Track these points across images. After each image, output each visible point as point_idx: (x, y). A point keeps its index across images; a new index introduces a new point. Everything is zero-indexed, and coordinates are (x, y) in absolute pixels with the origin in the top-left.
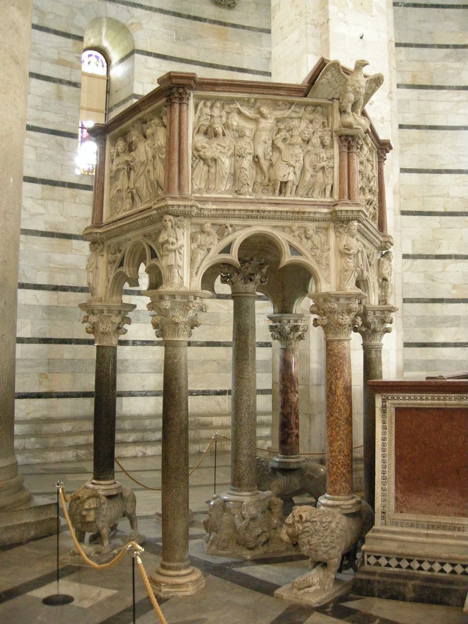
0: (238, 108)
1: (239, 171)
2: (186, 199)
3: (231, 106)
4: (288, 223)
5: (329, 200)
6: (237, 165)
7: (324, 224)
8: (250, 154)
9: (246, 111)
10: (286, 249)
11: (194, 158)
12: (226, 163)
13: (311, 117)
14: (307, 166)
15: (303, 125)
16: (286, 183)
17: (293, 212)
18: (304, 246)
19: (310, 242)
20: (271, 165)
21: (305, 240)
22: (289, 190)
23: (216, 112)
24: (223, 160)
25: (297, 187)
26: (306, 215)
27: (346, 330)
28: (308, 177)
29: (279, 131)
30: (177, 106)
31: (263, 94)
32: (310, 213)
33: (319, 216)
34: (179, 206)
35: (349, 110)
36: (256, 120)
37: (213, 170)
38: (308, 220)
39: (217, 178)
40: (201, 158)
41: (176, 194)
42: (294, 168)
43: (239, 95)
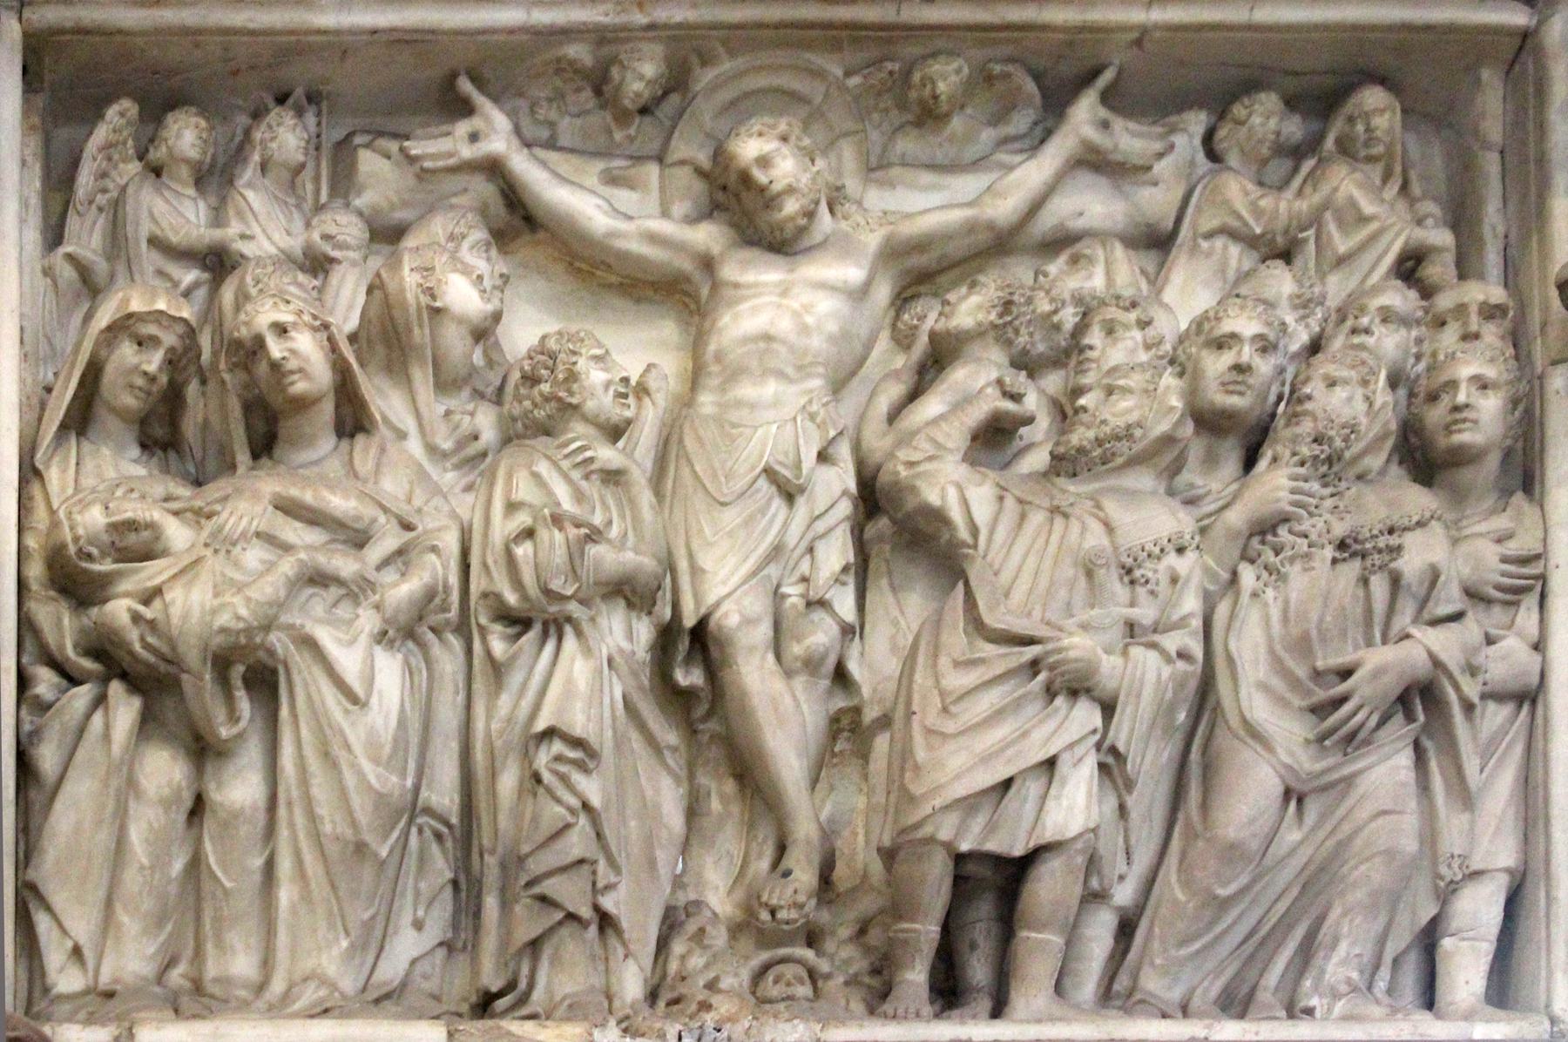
0: (494, 168)
1: (508, 781)
3: (415, 148)
6: (500, 714)
9: (578, 197)
12: (368, 693)
13: (1286, 206)
14: (1254, 695)
16: (1012, 874)
23: (264, 226)
29: (937, 360)
39: (285, 866)
40: (110, 661)
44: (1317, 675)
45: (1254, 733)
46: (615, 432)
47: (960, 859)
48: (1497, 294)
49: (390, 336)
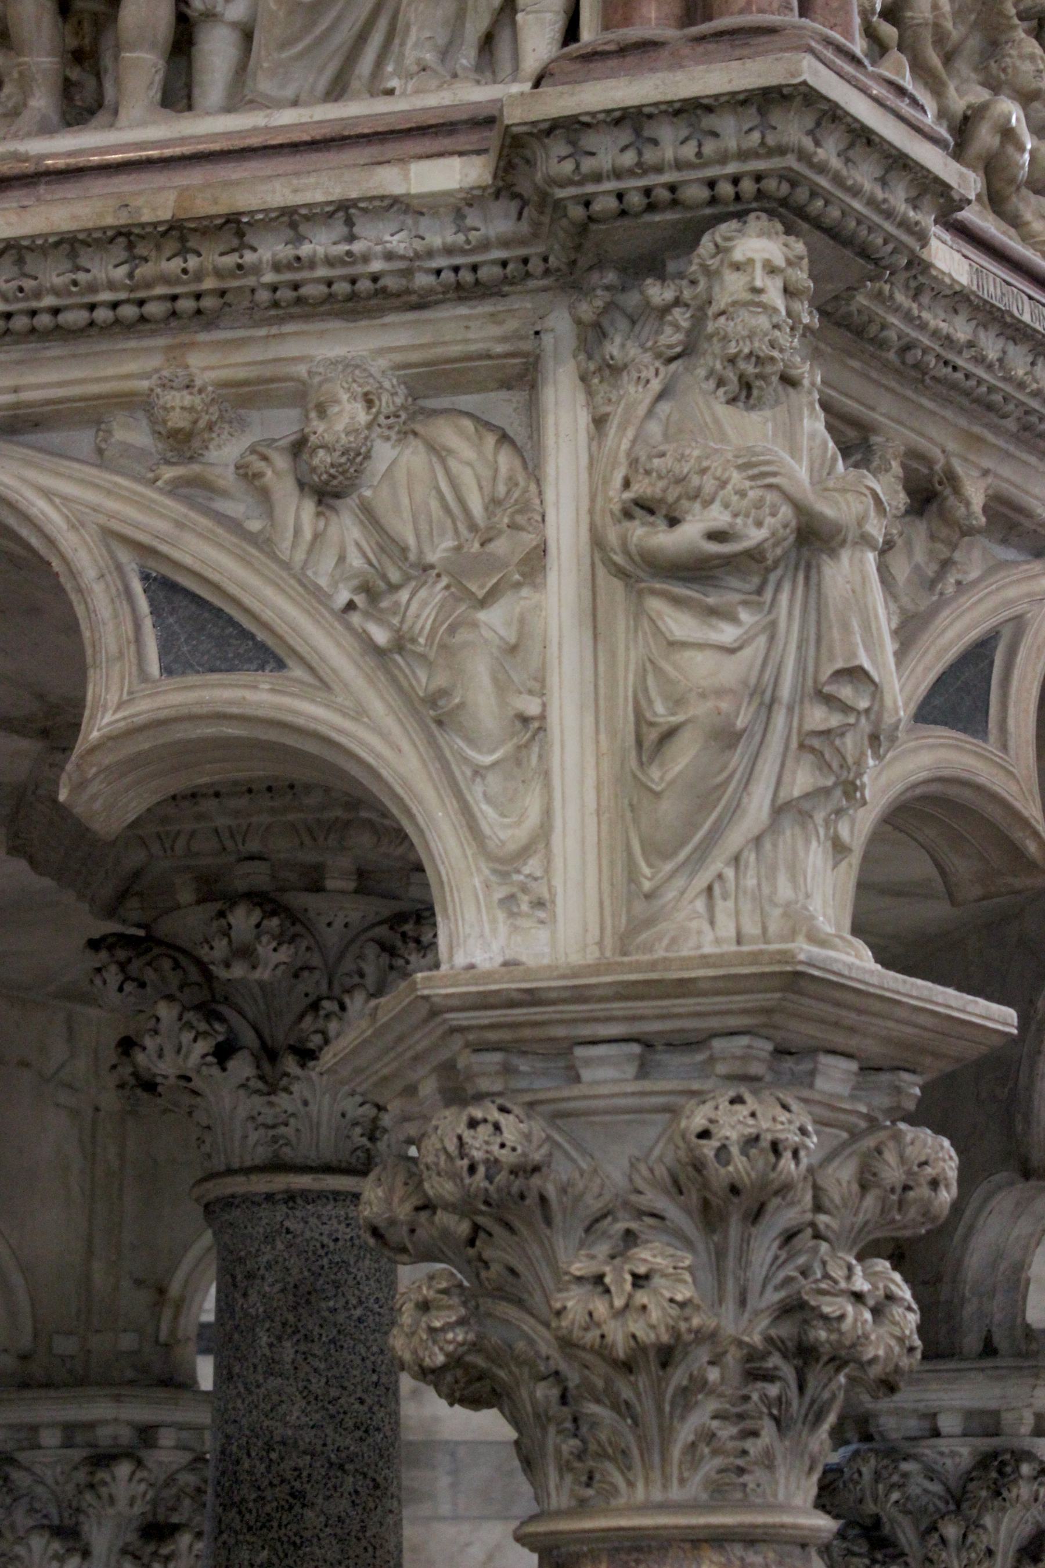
4: (128, 366)
7: (465, 330)
10: (115, 625)
17: (128, 238)
18: (293, 575)
19: (346, 528)
21: (297, 513)
22: (140, 67)
25: (247, 35)
26: (269, 249)
27: (701, 1416)
32: (293, 220)
33: (399, 242)
38: (296, 303)
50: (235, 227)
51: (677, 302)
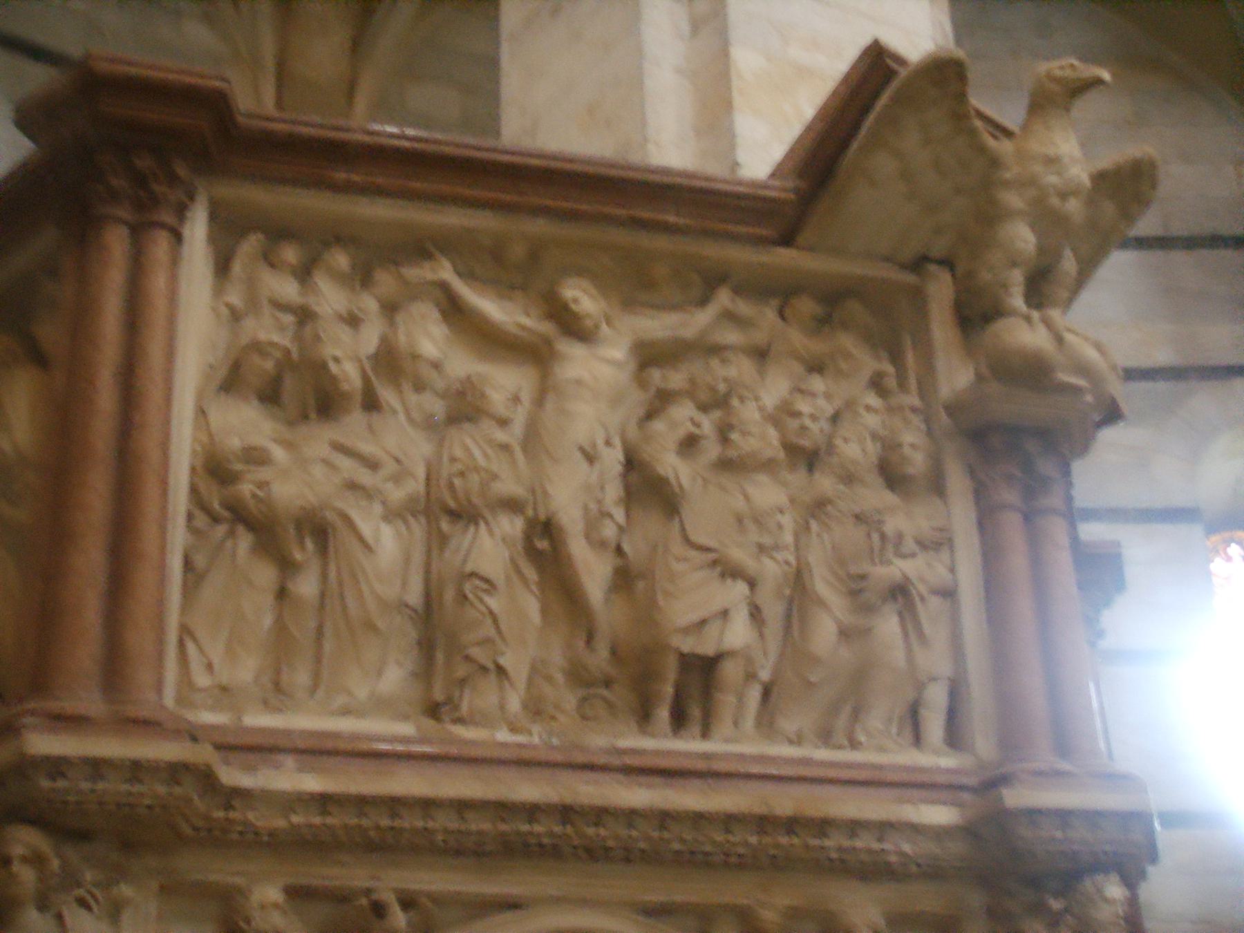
0: (444, 286)
1: (449, 595)
2: (147, 726)
5: (948, 761)
8: (512, 505)
11: (201, 520)
13: (817, 347)
14: (822, 585)
15: (774, 388)
20: (624, 578)
22: (726, 701)
24: (366, 528)
28: (824, 633)
29: (661, 401)
30: (116, 241)
31: (573, 216)
32: (854, 827)
33: (907, 848)
34: (97, 767)
35: (1017, 301)
36: (535, 354)
37: (306, 586)
40: (239, 515)
41: (90, 702)
42: (752, 584)
43: (453, 219)
44: (850, 576)
45: (821, 603)
46: (503, 423)
47: (682, 656)
48: (916, 402)
49: (390, 362)
50: (823, 826)
51: (1066, 910)
